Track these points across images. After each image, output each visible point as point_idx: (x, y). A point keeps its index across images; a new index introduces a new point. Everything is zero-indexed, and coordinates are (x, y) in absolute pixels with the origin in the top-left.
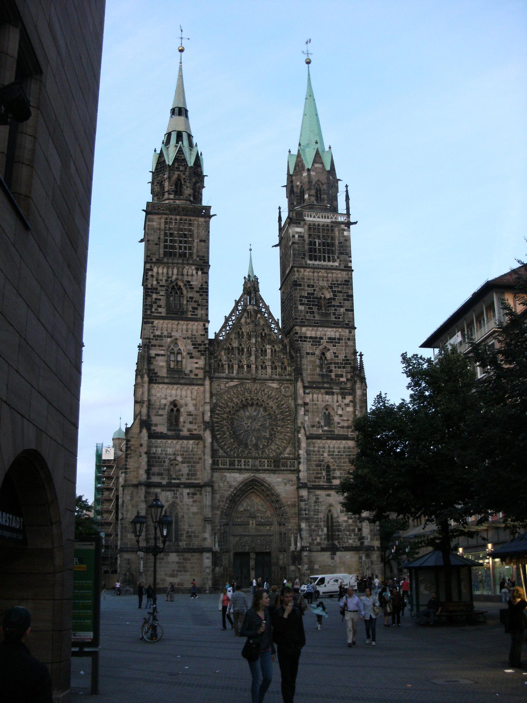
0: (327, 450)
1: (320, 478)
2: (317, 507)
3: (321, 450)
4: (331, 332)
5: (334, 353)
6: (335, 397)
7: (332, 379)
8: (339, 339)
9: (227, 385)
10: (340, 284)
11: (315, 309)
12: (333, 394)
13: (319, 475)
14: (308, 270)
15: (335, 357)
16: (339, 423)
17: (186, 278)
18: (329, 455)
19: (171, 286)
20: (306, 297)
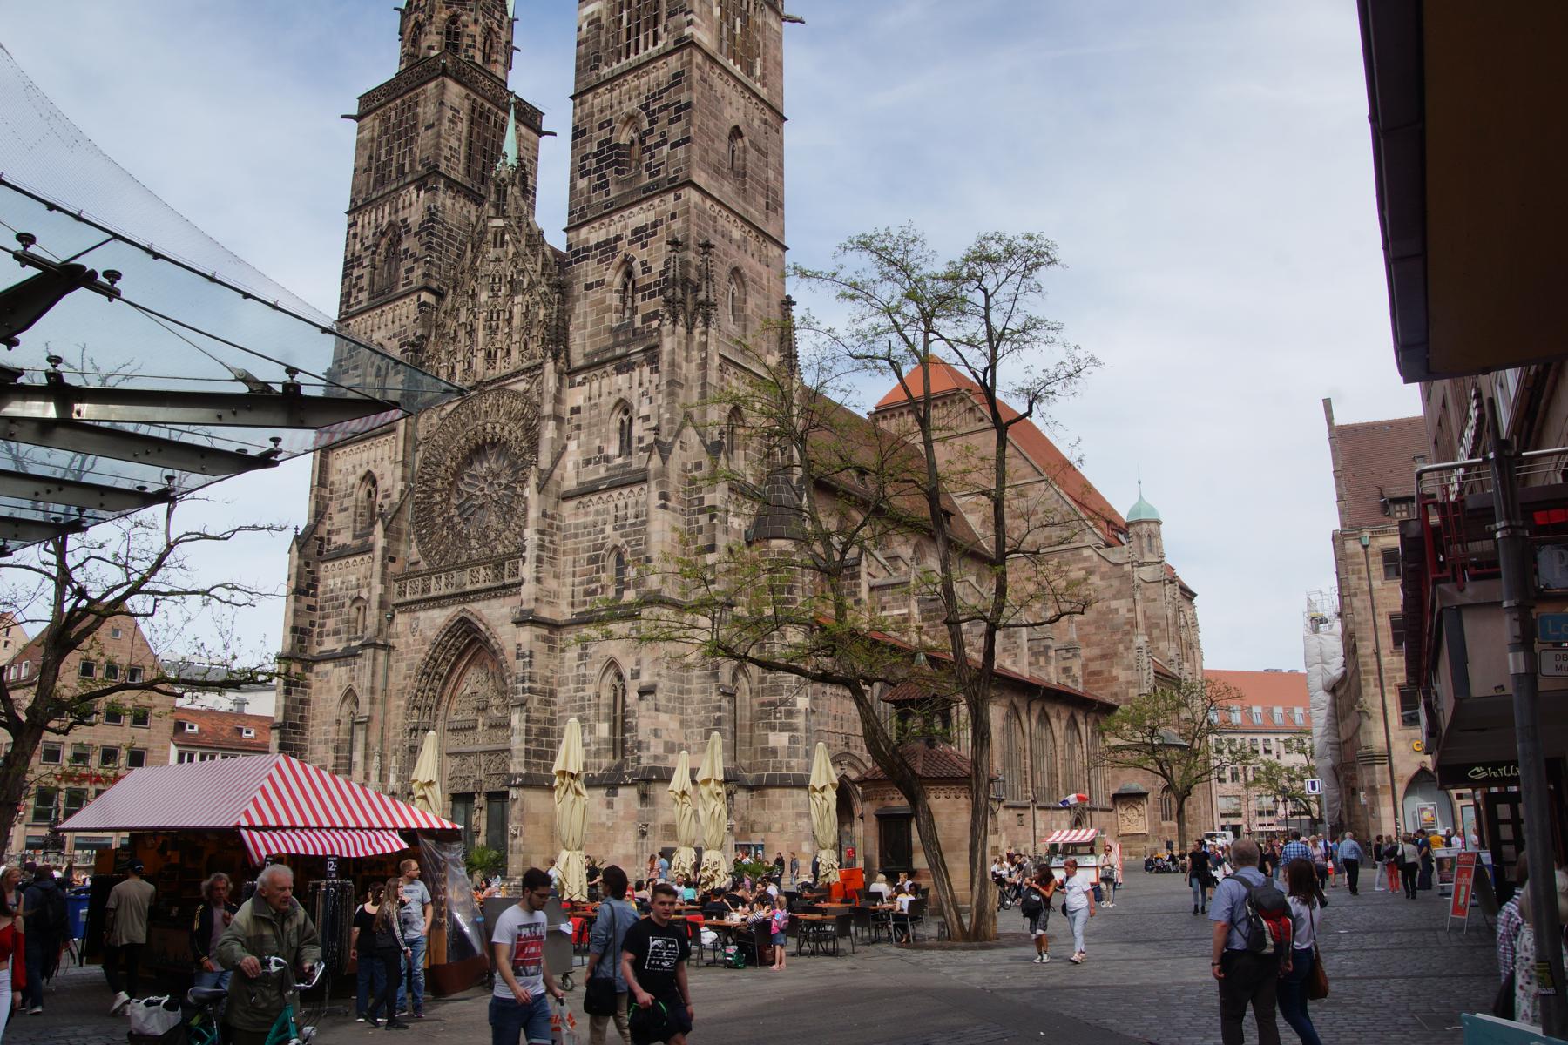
0: (611, 519)
1: (594, 592)
2: (582, 670)
3: (600, 518)
4: (639, 216)
5: (644, 264)
6: (636, 374)
7: (634, 332)
8: (655, 225)
9: (443, 414)
10: (666, 90)
11: (611, 175)
12: (630, 367)
13: (593, 586)
14: (600, 90)
15: (644, 272)
16: (641, 440)
17: (401, 215)
18: (615, 529)
19: (384, 242)
20: (595, 155)
